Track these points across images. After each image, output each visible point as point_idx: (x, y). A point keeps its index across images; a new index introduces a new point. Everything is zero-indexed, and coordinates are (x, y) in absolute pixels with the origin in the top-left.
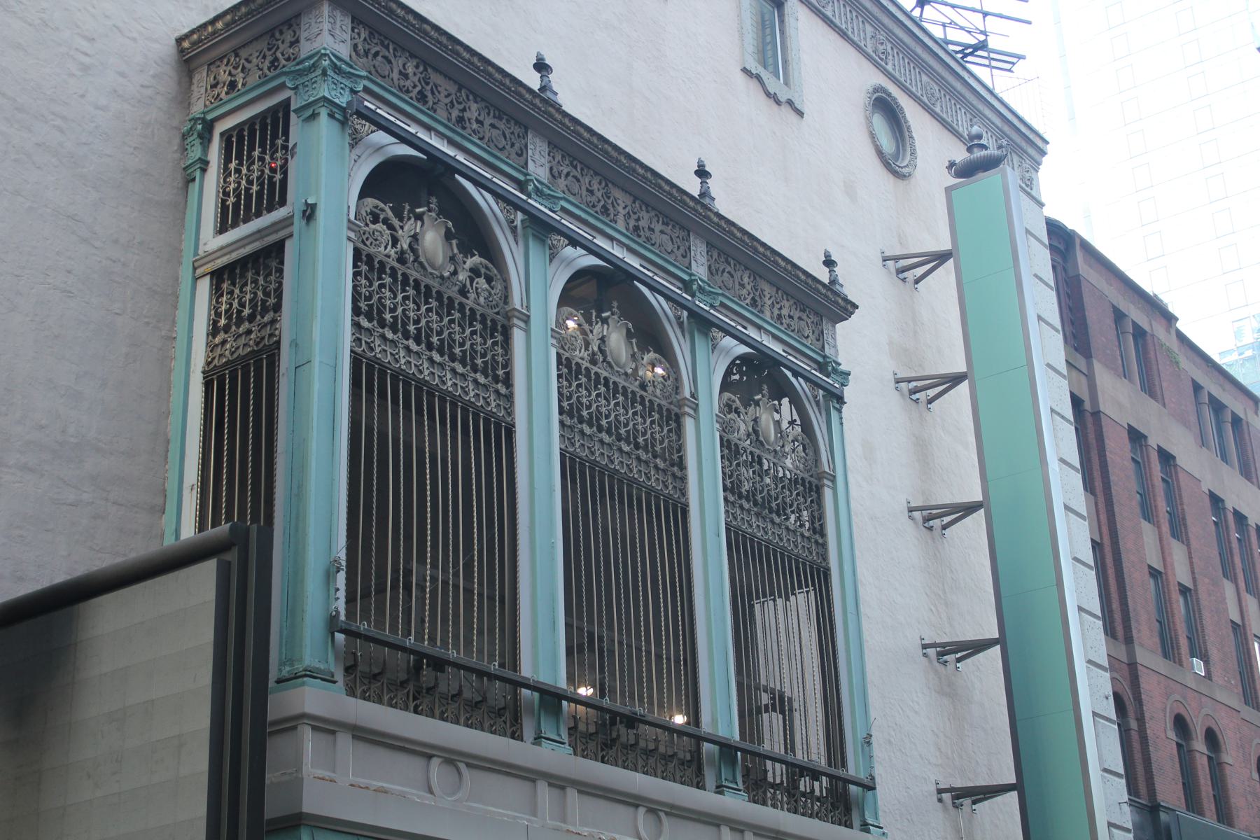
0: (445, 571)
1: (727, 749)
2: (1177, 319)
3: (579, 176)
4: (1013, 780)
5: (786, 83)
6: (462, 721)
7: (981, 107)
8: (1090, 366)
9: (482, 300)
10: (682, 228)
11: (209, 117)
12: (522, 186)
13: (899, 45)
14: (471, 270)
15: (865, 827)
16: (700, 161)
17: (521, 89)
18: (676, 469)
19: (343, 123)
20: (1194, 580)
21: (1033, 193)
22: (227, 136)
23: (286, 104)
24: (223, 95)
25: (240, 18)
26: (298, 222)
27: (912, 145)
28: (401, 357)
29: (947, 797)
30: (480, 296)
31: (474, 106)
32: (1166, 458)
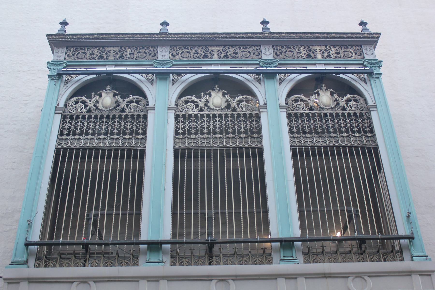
9: (353, 109)
12: (363, 64)
14: (346, 101)
30: (352, 108)
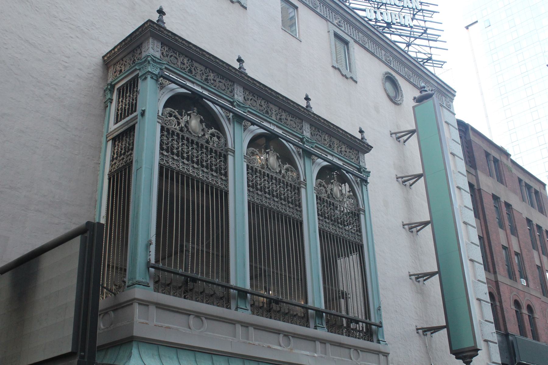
0: (198, 244)
1: (319, 313)
2: (510, 155)
3: (256, 100)
4: (445, 324)
5: (350, 71)
6: (205, 301)
7: (429, 79)
8: (476, 172)
9: (215, 145)
10: (300, 119)
11: (113, 83)
12: (232, 103)
13: (395, 57)
14: (211, 134)
15: (379, 342)
16: (306, 94)
17: (230, 68)
18: (297, 207)
19: (157, 81)
20: (521, 250)
21: (451, 110)
22: (119, 89)
24: (118, 75)
27: (402, 93)
28: (180, 166)
29: (420, 331)
31: (212, 75)
32: (508, 206)
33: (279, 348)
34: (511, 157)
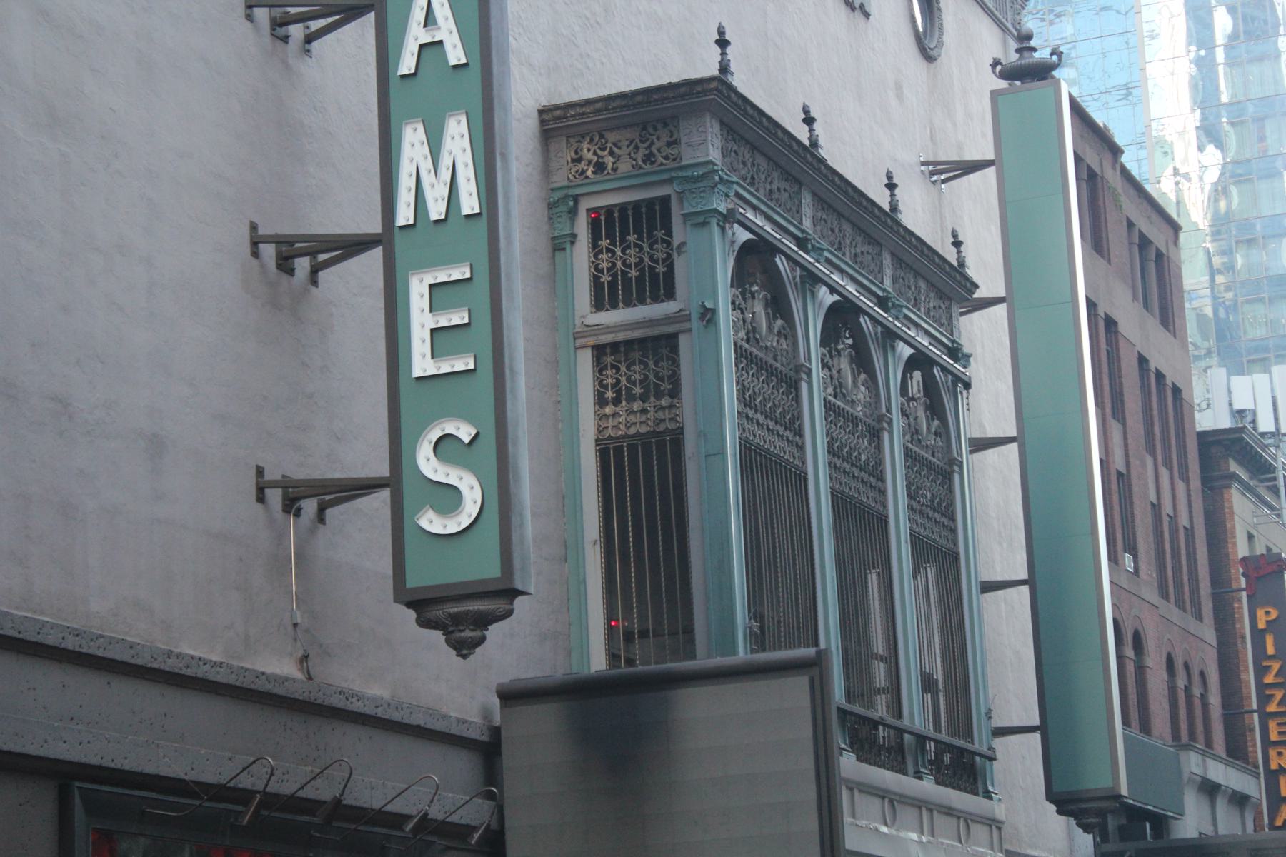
2: (1122, 152)
4: (1036, 721)
15: (988, 795)
23: (665, 201)
24: (589, 173)
25: (614, 108)
26: (695, 324)
27: (940, 19)
28: (761, 438)
33: (884, 829)
34: (1125, 159)
